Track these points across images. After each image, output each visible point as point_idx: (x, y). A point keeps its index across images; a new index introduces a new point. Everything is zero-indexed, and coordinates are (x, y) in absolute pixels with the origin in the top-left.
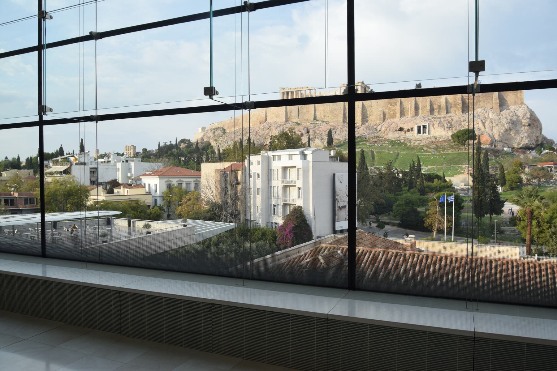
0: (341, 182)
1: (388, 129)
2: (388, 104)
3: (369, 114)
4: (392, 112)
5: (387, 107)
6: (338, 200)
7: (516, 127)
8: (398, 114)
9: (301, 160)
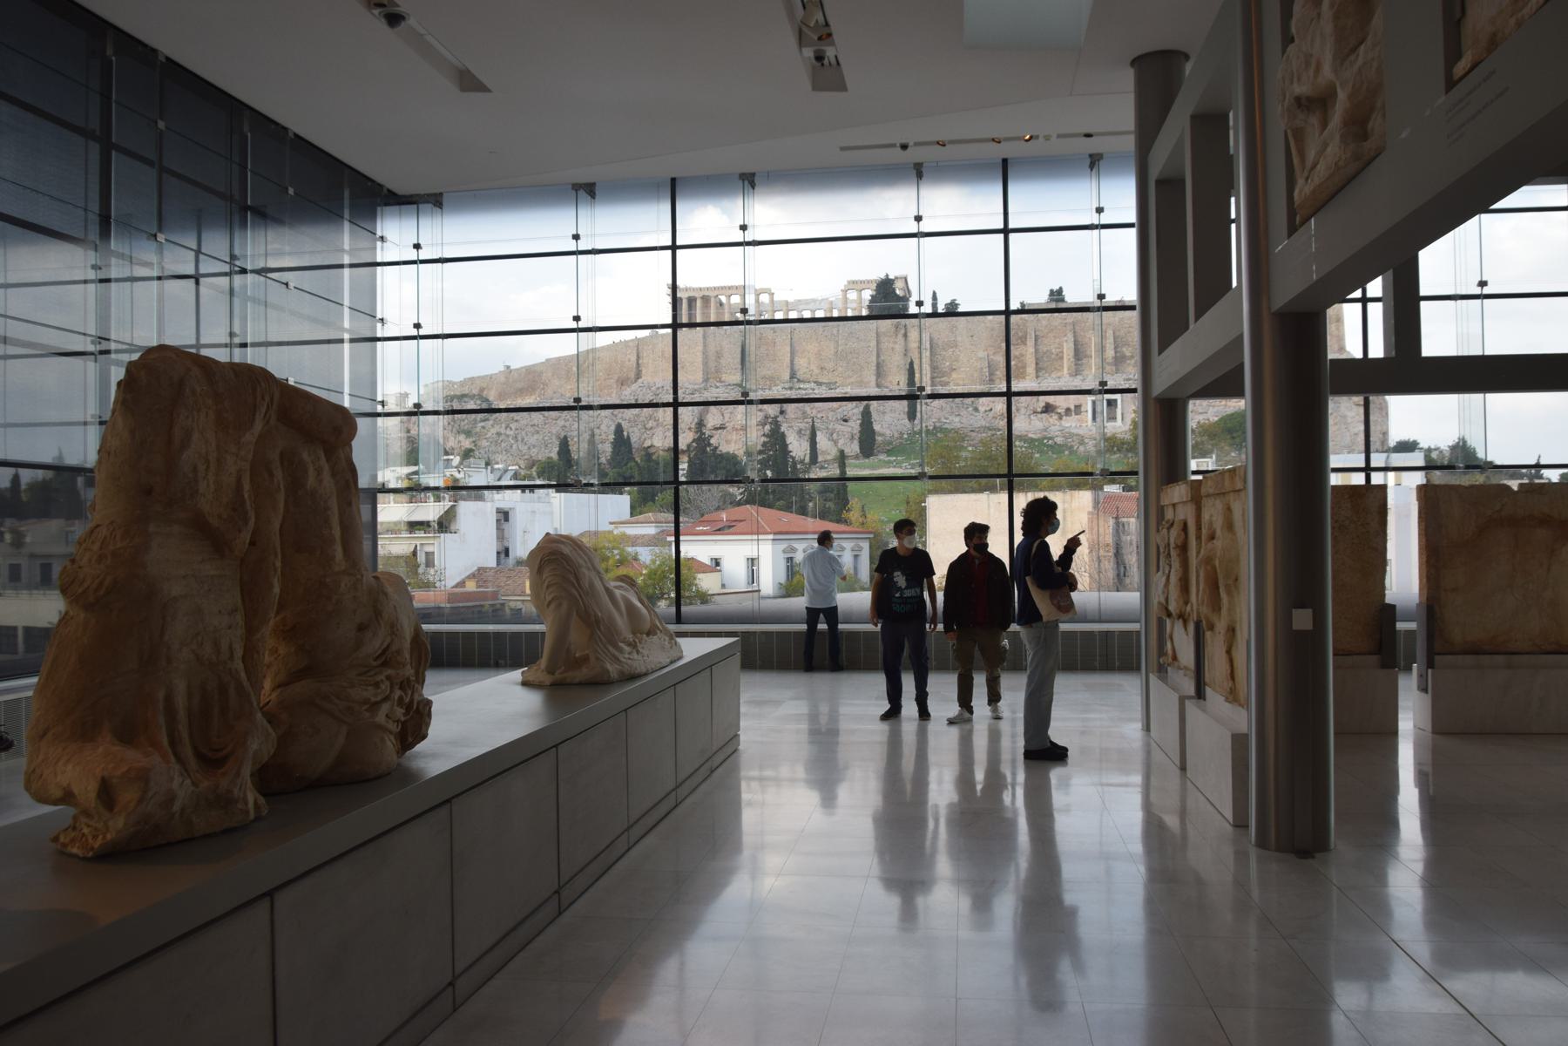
3: (951, 365)
7: (1338, 407)
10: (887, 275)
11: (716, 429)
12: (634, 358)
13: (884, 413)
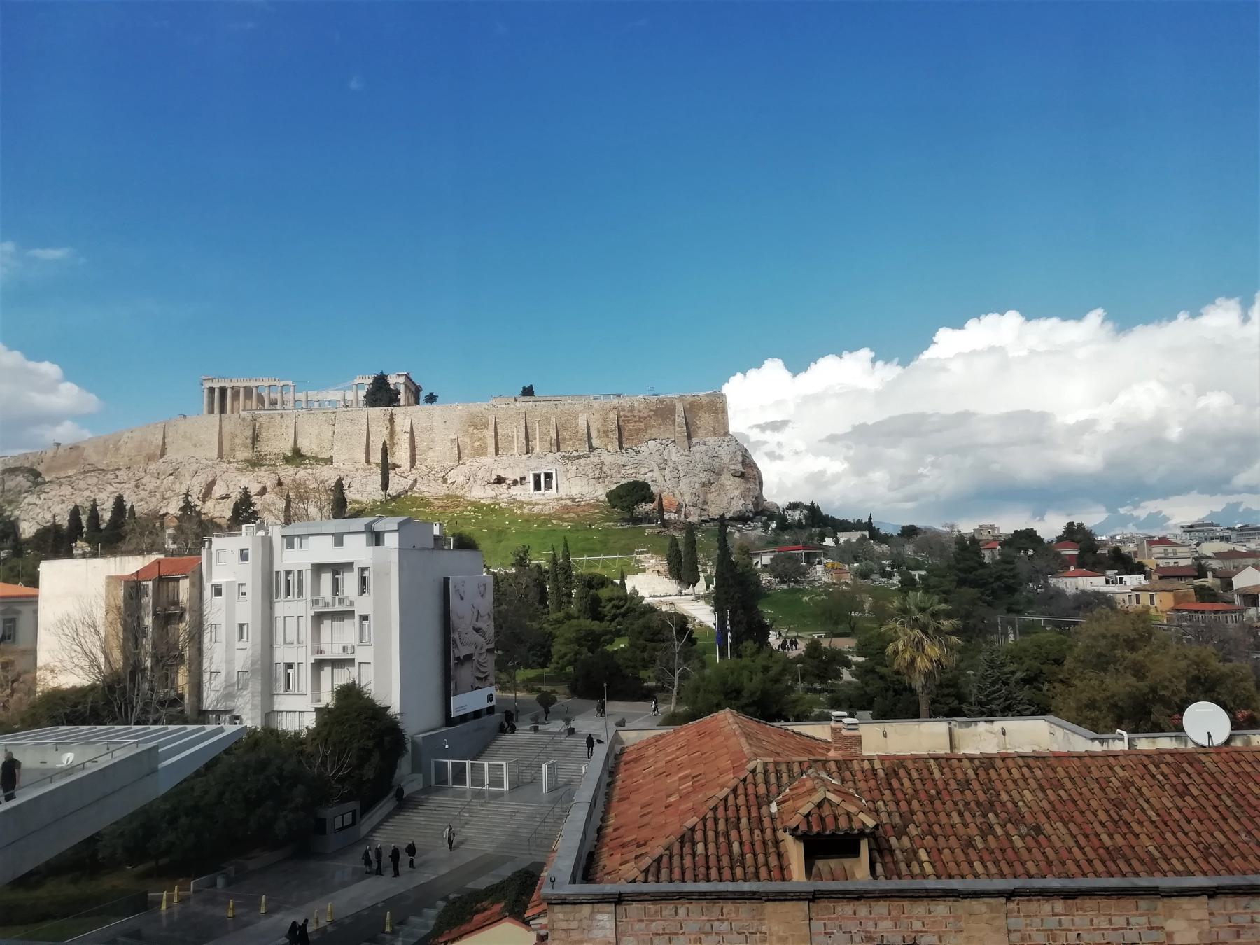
0: (462, 598)
1: (472, 480)
2: (470, 426)
4: (477, 444)
5: (468, 431)
6: (455, 641)
8: (491, 449)
9: (368, 545)
12: (161, 437)
13: (367, 484)
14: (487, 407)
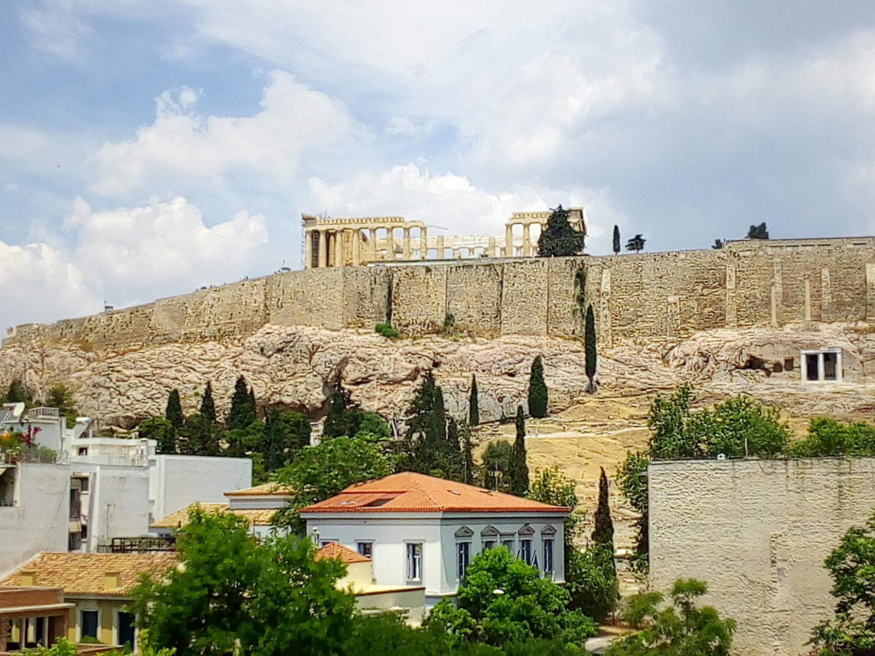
1: (711, 362)
4: (706, 310)
10: (560, 207)
11: (357, 384)
12: (261, 298)
14: (722, 255)
